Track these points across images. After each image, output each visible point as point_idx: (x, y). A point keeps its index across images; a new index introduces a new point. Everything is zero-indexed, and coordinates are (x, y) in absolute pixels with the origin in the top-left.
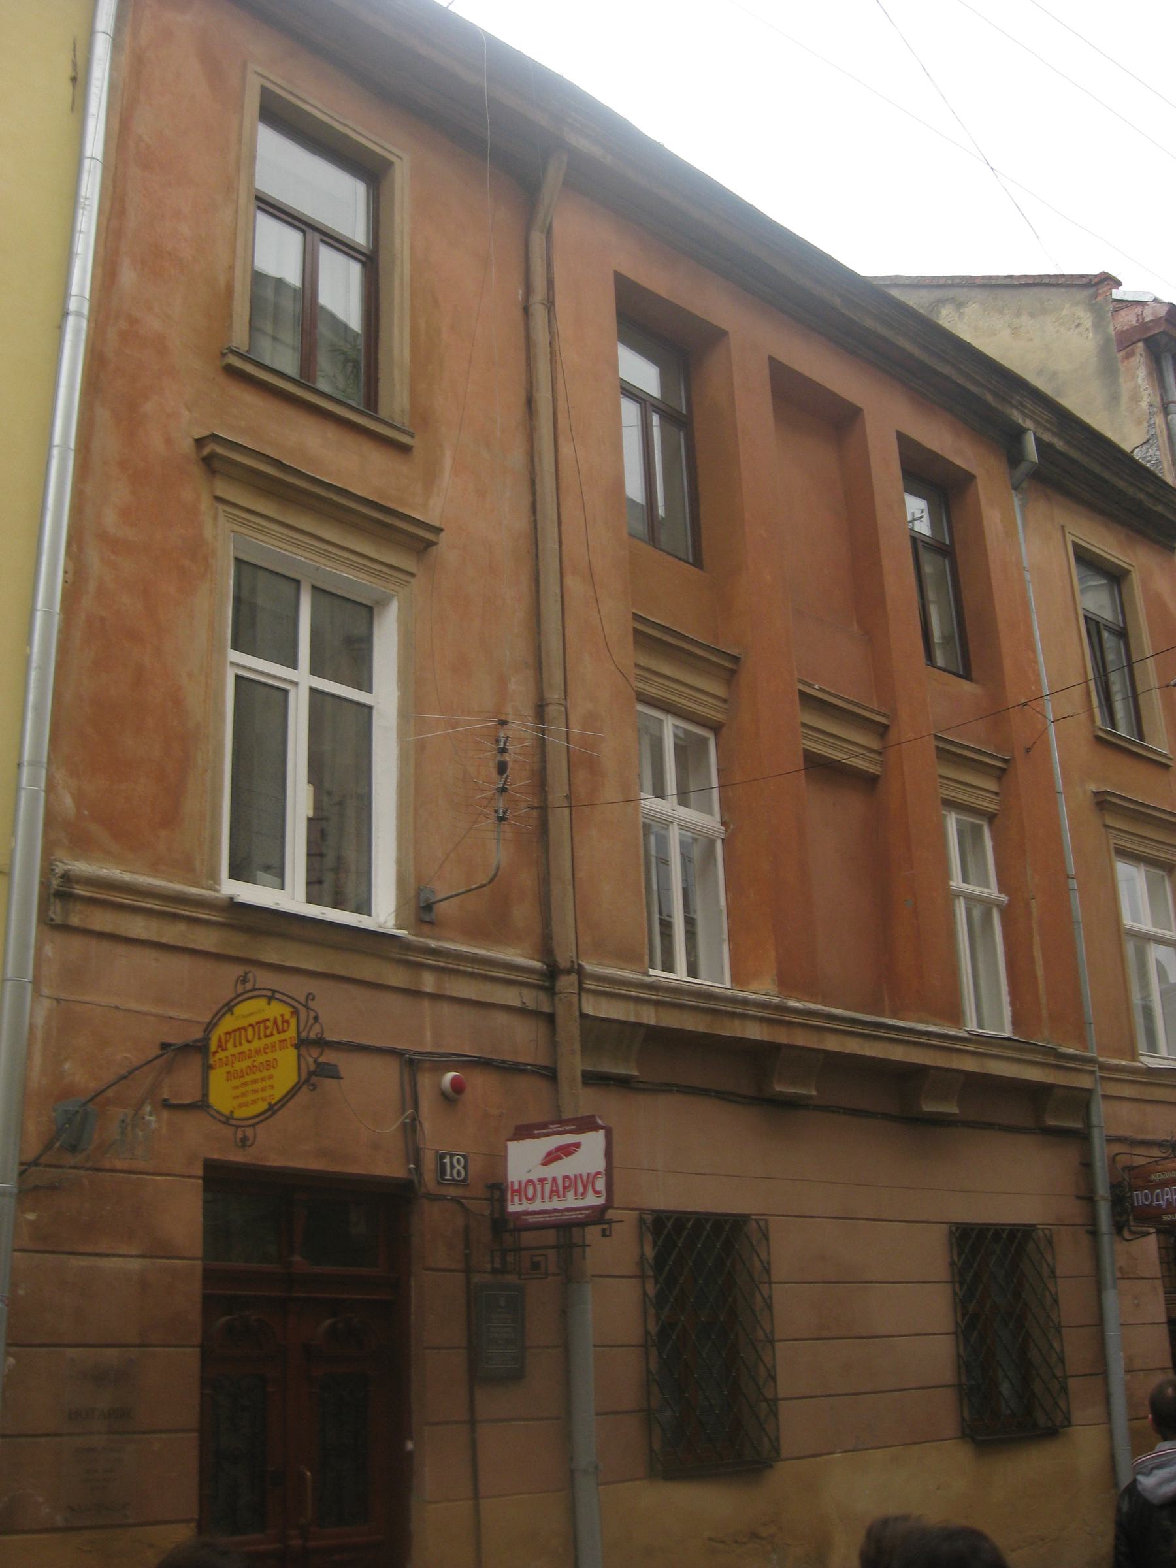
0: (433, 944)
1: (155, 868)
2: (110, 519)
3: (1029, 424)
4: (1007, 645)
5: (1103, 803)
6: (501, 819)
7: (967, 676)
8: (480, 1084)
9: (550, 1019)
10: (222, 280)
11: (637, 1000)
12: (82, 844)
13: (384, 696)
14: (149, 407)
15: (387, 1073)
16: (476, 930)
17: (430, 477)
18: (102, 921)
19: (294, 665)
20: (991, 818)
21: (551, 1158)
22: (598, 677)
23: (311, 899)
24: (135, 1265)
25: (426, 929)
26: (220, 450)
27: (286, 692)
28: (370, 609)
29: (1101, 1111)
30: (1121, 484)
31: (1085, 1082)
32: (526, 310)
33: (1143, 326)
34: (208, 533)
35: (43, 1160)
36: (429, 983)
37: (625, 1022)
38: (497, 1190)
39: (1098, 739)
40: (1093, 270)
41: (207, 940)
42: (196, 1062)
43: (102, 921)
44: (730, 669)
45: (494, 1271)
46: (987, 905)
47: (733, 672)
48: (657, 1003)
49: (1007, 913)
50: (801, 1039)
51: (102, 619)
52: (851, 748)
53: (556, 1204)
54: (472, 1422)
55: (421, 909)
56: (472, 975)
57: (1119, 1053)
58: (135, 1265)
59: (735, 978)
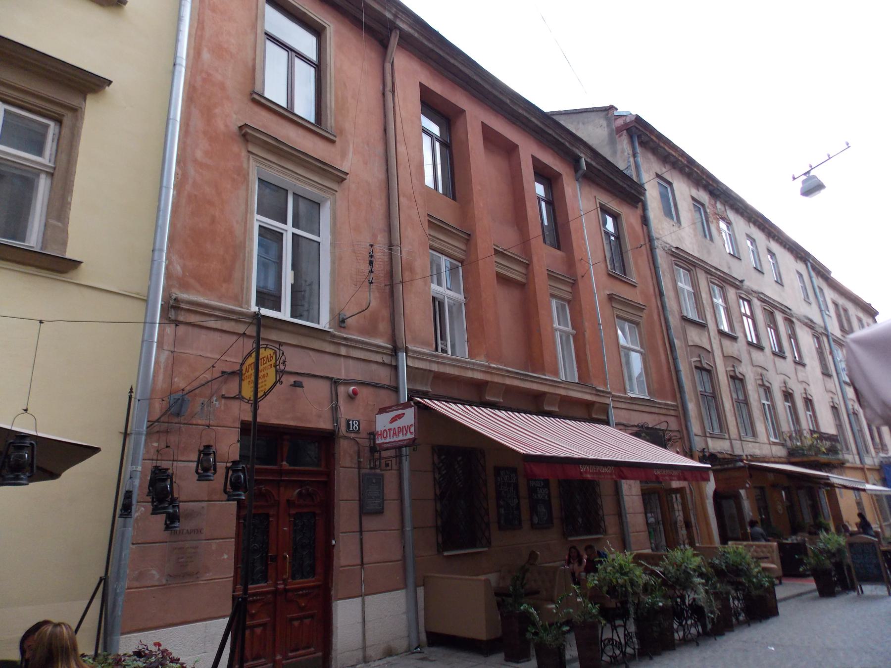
0: (345, 336)
1: (220, 299)
2: (199, 154)
3: (582, 155)
4: (574, 237)
5: (611, 298)
6: (371, 283)
7: (559, 248)
8: (364, 392)
9: (396, 368)
10: (250, 64)
11: (430, 361)
12: (184, 286)
13: (325, 238)
14: (217, 111)
15: (325, 386)
16: (363, 331)
17: (344, 155)
18: (193, 318)
19: (285, 223)
20: (569, 302)
21: (393, 420)
22: (413, 238)
23: (292, 316)
25: (342, 330)
26: (249, 131)
27: (282, 234)
28: (319, 204)
29: (612, 412)
30: (618, 181)
31: (607, 401)
32: (384, 94)
33: (626, 124)
34: (245, 165)
35: (162, 419)
36: (343, 351)
37: (425, 370)
38: (372, 435)
39: (609, 275)
40: (607, 105)
42: (237, 379)
43: (193, 318)
44: (468, 238)
45: (371, 468)
46: (568, 334)
47: (468, 240)
48: (438, 363)
49: (575, 337)
50: (496, 379)
51: (195, 196)
52: (515, 272)
54: (361, 532)
55: (341, 322)
56: (362, 349)
57: (619, 391)
59: (470, 356)
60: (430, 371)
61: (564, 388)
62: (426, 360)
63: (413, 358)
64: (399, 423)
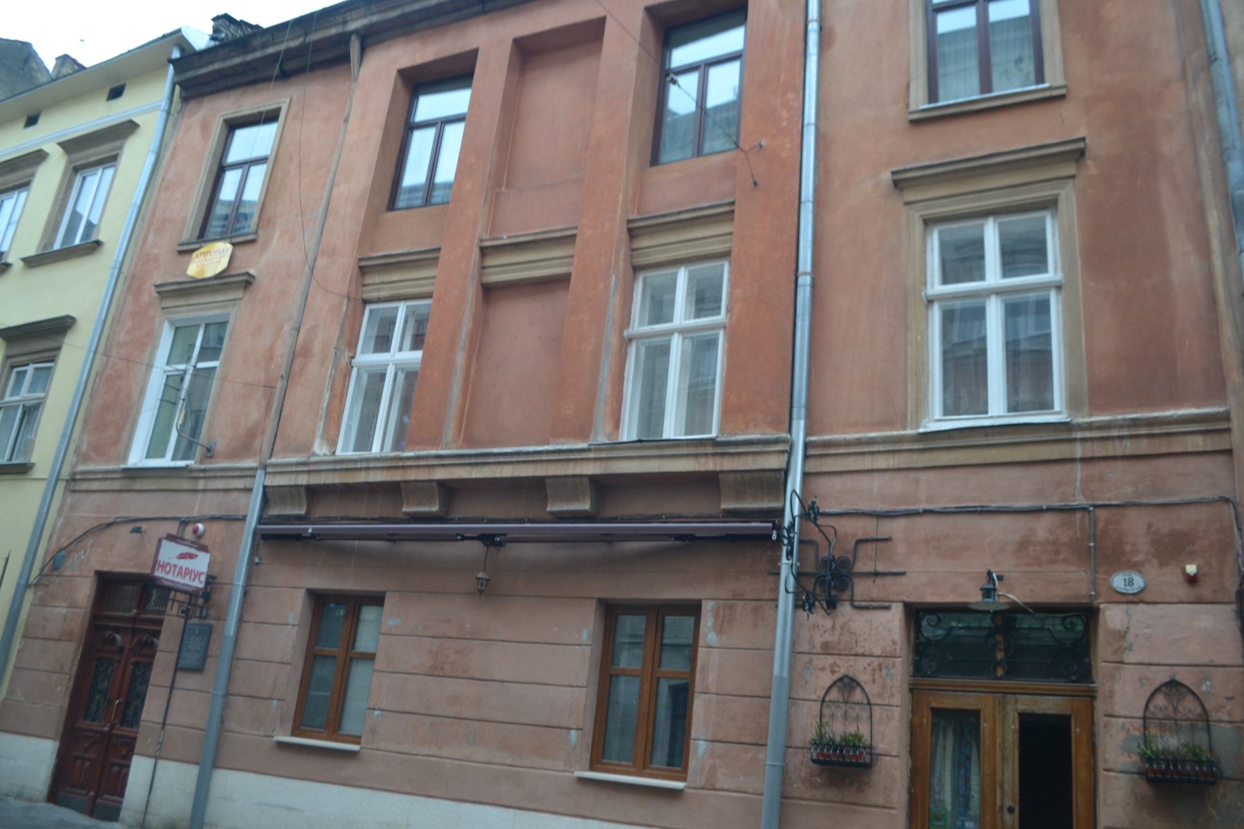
1: (107, 462)
11: (297, 472)
18: (85, 486)
24: (64, 611)
36: (201, 485)
37: (290, 486)
41: (116, 485)
43: (85, 486)
45: (201, 617)
48: (309, 472)
50: (412, 475)
53: (179, 579)
54: (172, 688)
58: (64, 611)
60: (297, 486)
61: (596, 459)
62: (291, 472)
63: (274, 473)
64: (185, 563)
